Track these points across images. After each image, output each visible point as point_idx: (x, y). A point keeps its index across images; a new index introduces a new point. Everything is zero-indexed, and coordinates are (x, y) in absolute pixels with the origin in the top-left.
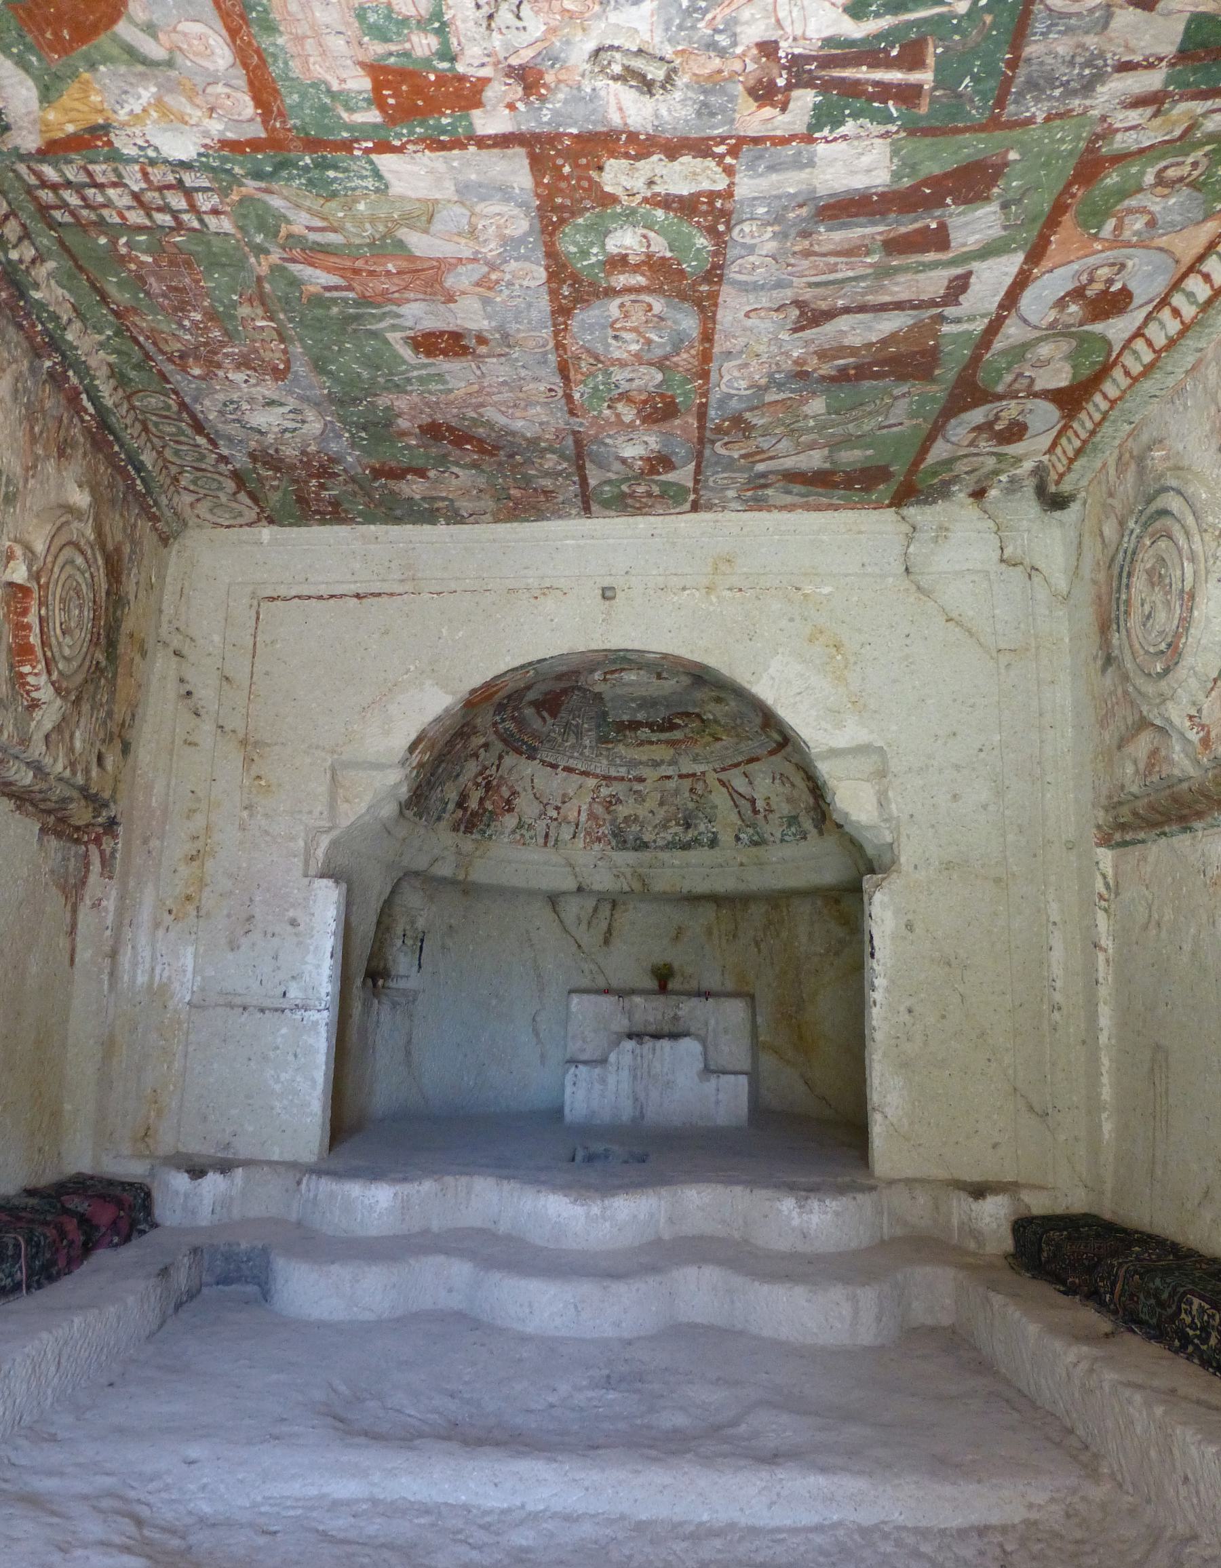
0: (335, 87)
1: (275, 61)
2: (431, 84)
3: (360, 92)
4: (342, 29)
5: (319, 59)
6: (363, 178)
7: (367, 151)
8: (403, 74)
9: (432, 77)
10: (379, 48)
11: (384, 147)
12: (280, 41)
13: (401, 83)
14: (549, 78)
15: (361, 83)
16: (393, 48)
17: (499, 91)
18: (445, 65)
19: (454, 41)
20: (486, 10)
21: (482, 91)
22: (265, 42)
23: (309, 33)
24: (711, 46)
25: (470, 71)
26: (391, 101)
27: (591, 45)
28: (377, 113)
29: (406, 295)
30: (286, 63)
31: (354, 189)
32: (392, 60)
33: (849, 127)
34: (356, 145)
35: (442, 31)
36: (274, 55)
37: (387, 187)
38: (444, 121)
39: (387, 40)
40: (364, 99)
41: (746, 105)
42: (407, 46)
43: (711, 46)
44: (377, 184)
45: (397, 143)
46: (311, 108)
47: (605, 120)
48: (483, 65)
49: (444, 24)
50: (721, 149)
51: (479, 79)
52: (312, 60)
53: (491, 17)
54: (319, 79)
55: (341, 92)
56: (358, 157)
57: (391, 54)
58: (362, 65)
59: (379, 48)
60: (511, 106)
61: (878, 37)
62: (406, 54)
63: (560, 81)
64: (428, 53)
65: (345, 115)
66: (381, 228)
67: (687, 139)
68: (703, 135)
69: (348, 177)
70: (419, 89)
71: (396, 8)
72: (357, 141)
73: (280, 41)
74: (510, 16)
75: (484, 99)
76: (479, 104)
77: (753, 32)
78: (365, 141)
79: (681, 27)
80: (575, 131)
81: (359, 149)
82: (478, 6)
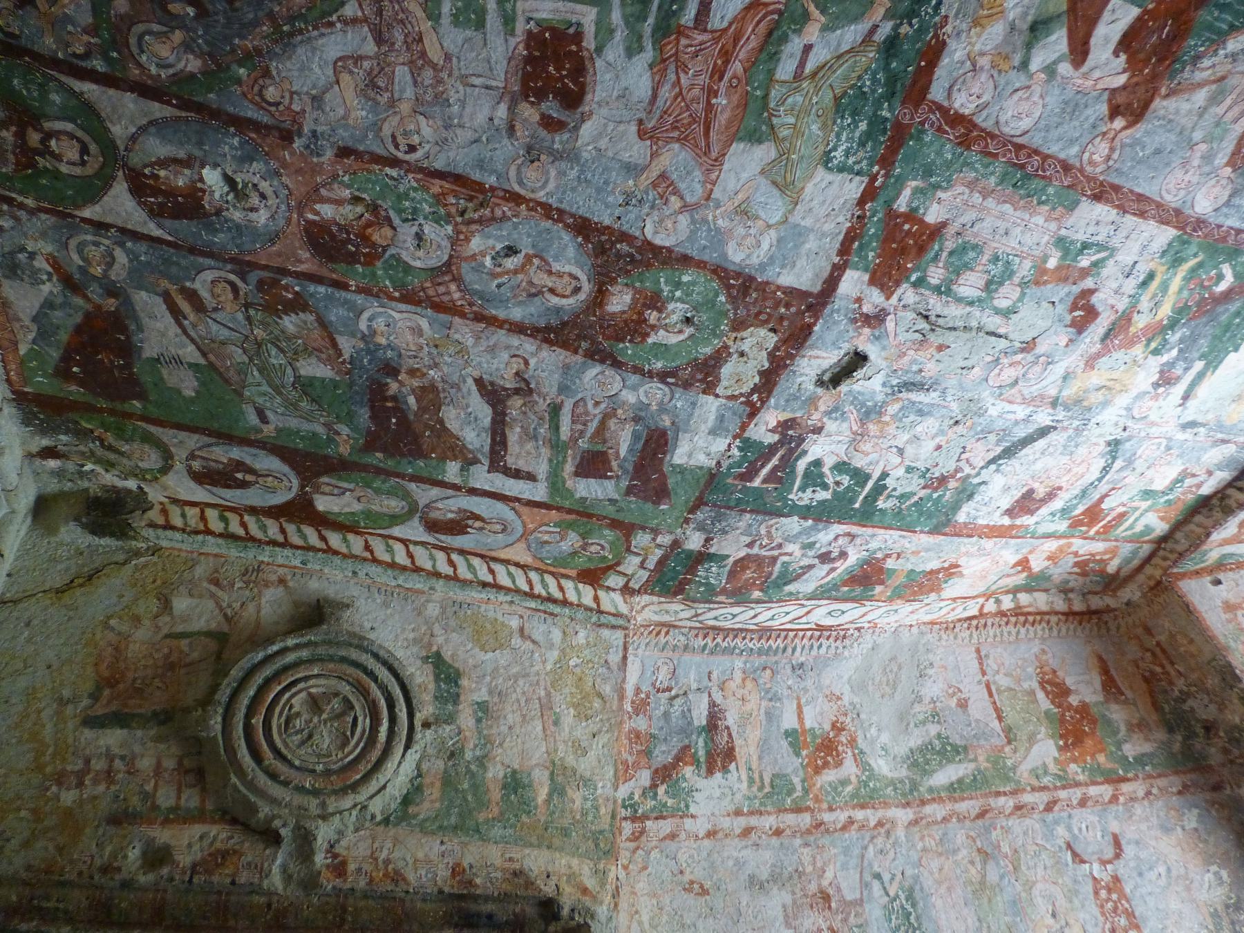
0: (940, 194)
1: (983, 165)
2: (905, 264)
3: (926, 209)
4: (975, 229)
5: (965, 197)
6: (847, 153)
7: (873, 178)
8: (921, 249)
9: (909, 266)
10: (950, 245)
11: (869, 194)
12: (993, 180)
13: (916, 243)
14: (867, 331)
15: (933, 215)
16: (945, 254)
17: (874, 299)
18: (913, 278)
19: (927, 293)
20: (933, 318)
21: (882, 290)
22: (999, 167)
23: (985, 204)
24: (836, 409)
25: (899, 291)
26: (907, 227)
27: (872, 356)
28: (902, 210)
29: (667, 87)
30: (976, 171)
31: (838, 136)
32: (936, 247)
33: (735, 452)
34: (882, 172)
35: (937, 290)
36: (986, 166)
37: (830, 169)
38: (871, 254)
39: (951, 253)
40: (917, 209)
41: (783, 417)
42: (941, 265)
43: (836, 409)
44: (835, 162)
45: (867, 207)
46: (933, 162)
47: (812, 347)
48: (900, 300)
49: (940, 293)
50: (755, 397)
51: (892, 293)
52: (967, 191)
53: (926, 317)
54: (952, 186)
55: (934, 195)
56: (872, 167)
57: (941, 250)
58: (944, 225)
59: (950, 245)
60: (859, 300)
61: (793, 471)
62: (936, 258)
63: (860, 334)
64: (929, 274)
65: (914, 184)
66: (784, 133)
67: (775, 385)
68: (775, 393)
69: (852, 138)
70: (903, 251)
71: (968, 273)
72: (887, 176)
73: (993, 180)
74: (920, 327)
75: (873, 288)
76: (872, 282)
77: (831, 426)
78: (883, 183)
79: (855, 398)
80: (816, 328)
81: (878, 173)
82: (938, 316)
